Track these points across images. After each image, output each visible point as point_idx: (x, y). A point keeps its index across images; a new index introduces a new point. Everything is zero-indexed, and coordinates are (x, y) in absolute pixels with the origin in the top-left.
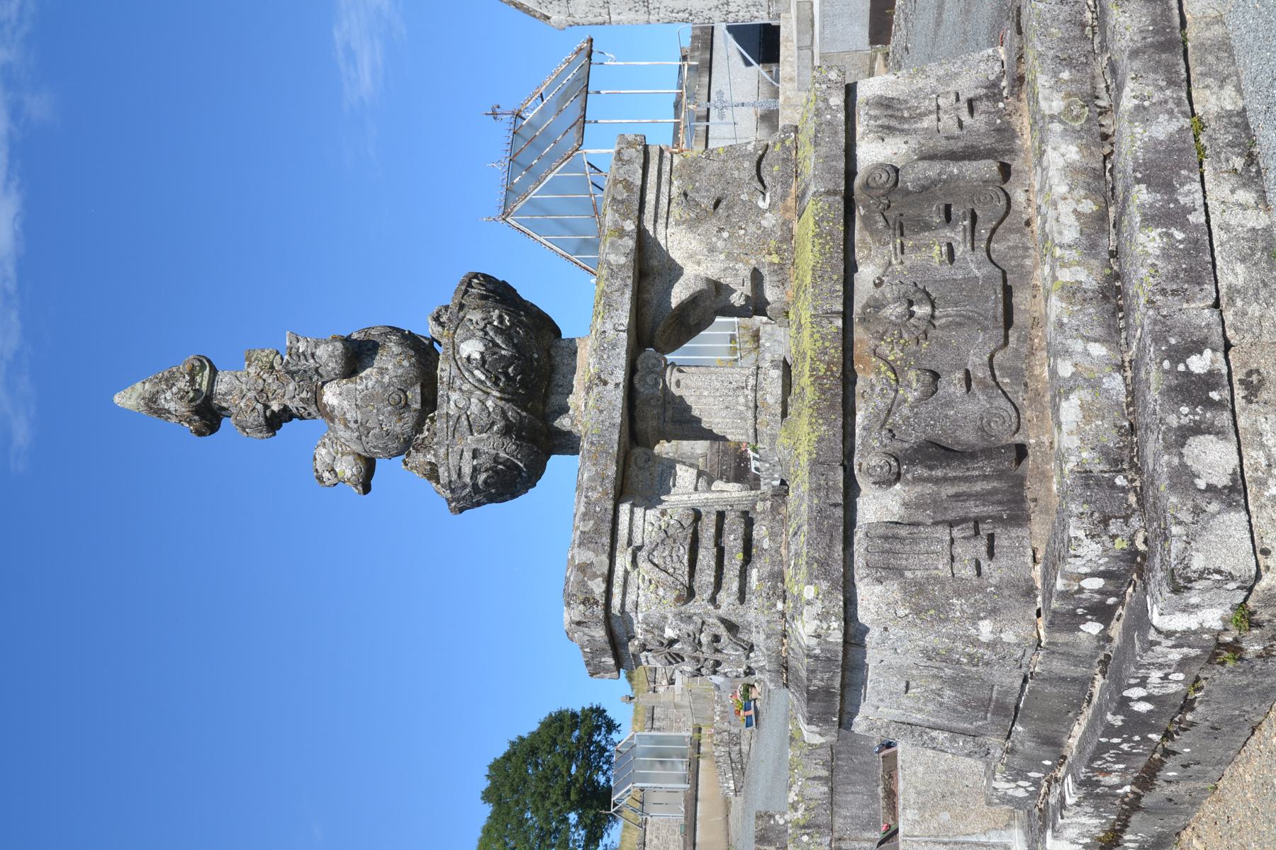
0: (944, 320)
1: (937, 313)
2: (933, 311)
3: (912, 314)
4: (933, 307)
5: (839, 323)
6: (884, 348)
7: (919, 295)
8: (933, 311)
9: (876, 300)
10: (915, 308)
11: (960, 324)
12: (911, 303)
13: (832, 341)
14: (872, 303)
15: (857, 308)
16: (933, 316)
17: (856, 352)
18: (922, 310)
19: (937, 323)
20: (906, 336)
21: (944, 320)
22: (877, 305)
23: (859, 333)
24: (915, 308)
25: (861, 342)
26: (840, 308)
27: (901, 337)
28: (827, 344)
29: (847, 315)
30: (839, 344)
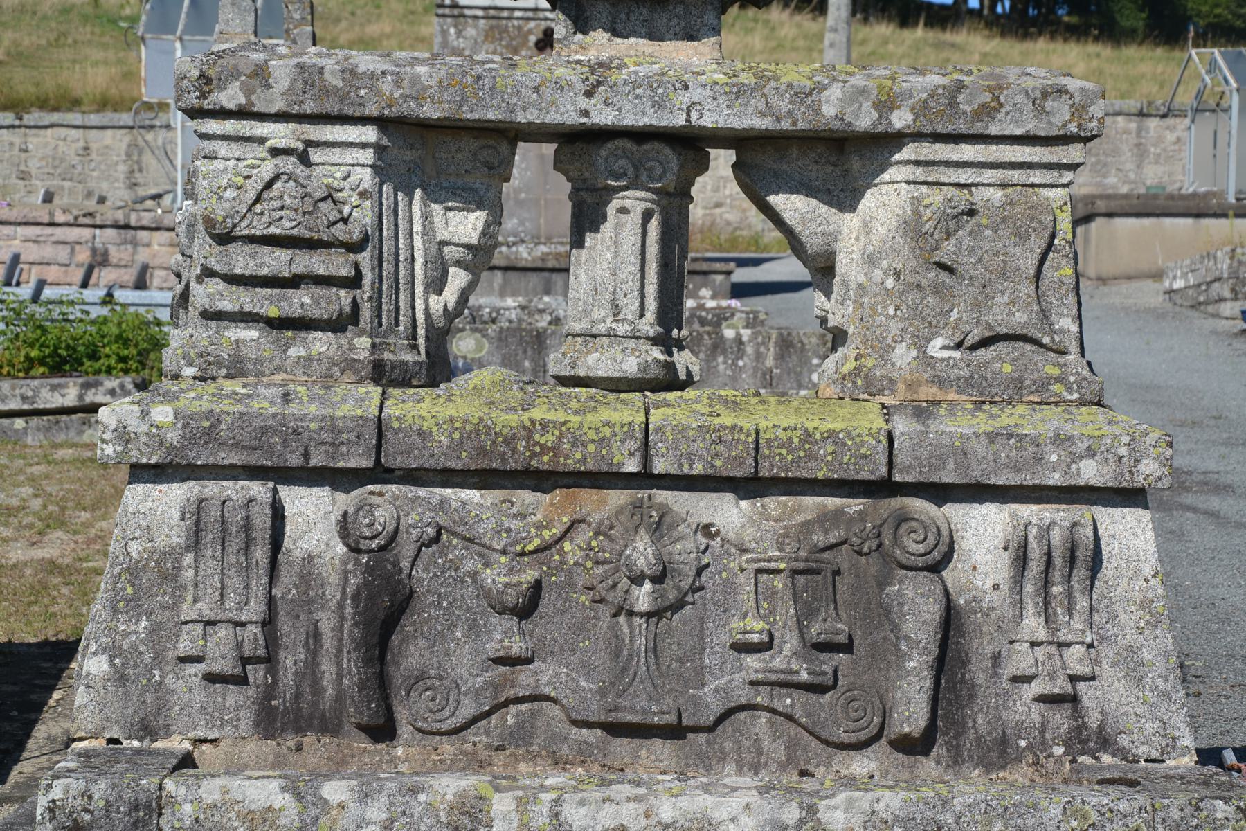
0: (626, 630)
1: (638, 620)
2: (642, 615)
3: (637, 580)
4: (648, 615)
5: (632, 466)
6: (583, 535)
7: (672, 595)
8: (642, 615)
9: (673, 526)
10: (648, 586)
11: (617, 654)
12: (658, 580)
13: (598, 456)
14: (668, 519)
15: (663, 496)
16: (631, 614)
17: (584, 494)
18: (643, 598)
19: (622, 619)
20: (600, 570)
21: (626, 630)
22: (661, 527)
23: (618, 498)
24: (648, 586)
25: (602, 502)
26: (659, 467)
27: (597, 563)
28: (591, 448)
29: (646, 478)
30: (591, 465)
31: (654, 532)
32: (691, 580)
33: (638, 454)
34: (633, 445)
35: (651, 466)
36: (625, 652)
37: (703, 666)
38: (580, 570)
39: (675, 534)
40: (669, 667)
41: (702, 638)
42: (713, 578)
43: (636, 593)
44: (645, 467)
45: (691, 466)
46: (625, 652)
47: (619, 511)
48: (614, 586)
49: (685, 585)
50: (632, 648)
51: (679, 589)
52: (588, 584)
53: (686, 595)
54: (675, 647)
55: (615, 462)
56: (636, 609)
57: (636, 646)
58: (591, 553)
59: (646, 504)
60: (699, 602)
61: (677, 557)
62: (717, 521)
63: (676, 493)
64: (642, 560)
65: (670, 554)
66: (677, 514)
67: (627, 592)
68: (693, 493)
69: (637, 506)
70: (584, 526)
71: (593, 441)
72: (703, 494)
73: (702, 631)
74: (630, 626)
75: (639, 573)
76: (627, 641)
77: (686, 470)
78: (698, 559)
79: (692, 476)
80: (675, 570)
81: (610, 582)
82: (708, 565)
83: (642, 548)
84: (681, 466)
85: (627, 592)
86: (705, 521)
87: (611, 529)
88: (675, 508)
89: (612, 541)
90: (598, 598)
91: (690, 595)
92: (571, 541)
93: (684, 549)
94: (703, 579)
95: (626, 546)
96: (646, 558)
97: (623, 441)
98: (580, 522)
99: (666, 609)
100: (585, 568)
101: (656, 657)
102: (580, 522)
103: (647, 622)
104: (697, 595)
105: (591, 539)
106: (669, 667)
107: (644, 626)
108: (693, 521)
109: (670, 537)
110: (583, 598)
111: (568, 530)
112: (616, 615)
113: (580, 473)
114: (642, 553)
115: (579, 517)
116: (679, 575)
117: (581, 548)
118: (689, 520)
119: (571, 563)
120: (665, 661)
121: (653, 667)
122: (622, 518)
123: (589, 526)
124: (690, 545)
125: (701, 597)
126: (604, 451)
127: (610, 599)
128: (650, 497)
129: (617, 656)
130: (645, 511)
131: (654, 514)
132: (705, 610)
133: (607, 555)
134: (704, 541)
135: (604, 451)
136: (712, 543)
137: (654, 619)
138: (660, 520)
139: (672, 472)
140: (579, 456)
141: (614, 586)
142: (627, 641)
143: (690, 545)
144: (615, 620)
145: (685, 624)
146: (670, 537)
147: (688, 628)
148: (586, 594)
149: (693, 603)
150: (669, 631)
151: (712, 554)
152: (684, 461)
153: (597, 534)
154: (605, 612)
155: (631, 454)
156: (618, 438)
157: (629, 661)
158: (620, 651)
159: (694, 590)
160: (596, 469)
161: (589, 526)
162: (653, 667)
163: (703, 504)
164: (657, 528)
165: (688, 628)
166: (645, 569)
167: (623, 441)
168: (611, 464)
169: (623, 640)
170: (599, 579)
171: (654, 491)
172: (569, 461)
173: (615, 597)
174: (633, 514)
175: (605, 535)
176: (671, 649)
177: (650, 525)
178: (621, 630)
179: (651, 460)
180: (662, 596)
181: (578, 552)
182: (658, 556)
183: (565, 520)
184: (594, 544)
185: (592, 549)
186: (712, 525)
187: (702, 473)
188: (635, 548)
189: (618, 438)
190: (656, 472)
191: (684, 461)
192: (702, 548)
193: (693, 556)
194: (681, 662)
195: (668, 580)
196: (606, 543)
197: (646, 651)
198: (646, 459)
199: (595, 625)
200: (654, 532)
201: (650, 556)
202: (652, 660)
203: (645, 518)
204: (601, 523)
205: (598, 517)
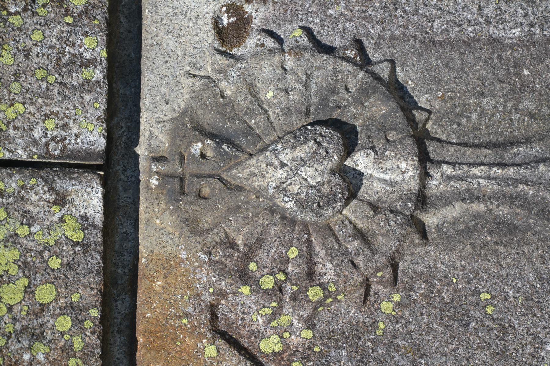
0: (455, 211)
1: (435, 184)
2: (425, 175)
3: (352, 182)
4: (424, 158)
5: (90, 198)
6: (247, 308)
7: (380, 107)
8: (425, 175)
9: (225, 107)
10: (361, 161)
11: (507, 230)
12: (350, 139)
13: (63, 279)
14: (209, 118)
15: (154, 130)
16: (422, 200)
17: (147, 312)
18: (386, 172)
19: (431, 219)
20: (327, 269)
21: (455, 211)
22: (227, 134)
23: (158, 230)
24: (361, 161)
25: (168, 266)
26: (92, 136)
27: (311, 275)
28: (45, 293)
29: (115, 167)
30: (87, 293)
31: (239, 148)
32: (345, 66)
33: (61, 184)
34: (38, 195)
35: (89, 154)
36: (504, 211)
37: (528, 42)
38: (324, 314)
39: (243, 101)
40: (532, 116)
41: (469, 43)
42: (335, 20)
43: (377, 186)
44: (92, 169)
45: (88, 64)
46: (504, 211)
47: (192, 227)
48: (361, 235)
49: (356, 79)
50: (499, 197)
51: (365, 91)
52: (358, 294)
53: (378, 78)
54: (488, 103)
55: (79, 236)
56: (414, 186)
57: (491, 187)
58: (288, 288)
59: (175, 167)
60: (388, 51)
61: (294, 97)
62: (213, 8)
63: (145, 102)
64: (308, 172)
65: (287, 111)
66: (197, 96)
67: (374, 207)
68: (145, 64)
69: (178, 187)
70: (224, 307)
71: (29, 290)
72: (147, 39)
73: (453, 44)
74: (446, 200)
75: (337, 180)
76: (479, 207)
77: (97, 74)
78: (297, 51)
79: (111, 58)
80: (323, 103)
81: (353, 245)
82: (308, 31)
83: (281, 174)
84: (87, 86)
85: (374, 207)
86: (208, 37)
87: (233, 245)
88: (181, 102)
89: (260, 241)
90: (387, 274)
91: (377, 69)
92: (258, 335)
93: (275, 82)
94: (337, 42)
95: (272, 210)
96: (303, 162)
97: (29, 219)
98: (214, 317)
99: (412, 121)
100: (321, 303)
101: (514, 143)
102: (214, 317)
103: (438, 163)
104: (374, 55)
105: (257, 289)
106: (532, 116)
107: (448, 170)
108: (209, 64)
109: (249, 112)
110: (387, 307)
111: (234, 343)
112: (423, 232)
113: (105, 319)
114: (290, 173)
115: (205, 318)
116: (334, 91)
117: (277, 313)
118: (209, 71)
119: (308, 334)
120: (520, 125)
121: (537, 150)
122: (206, 221)
123: (223, 294)
124: (266, 69)
125: (378, 46)
126: (55, 263)
127: (393, 244)
128: (158, 159)
129: (513, 229)
130: (191, 168)
131: (197, 148)
132: (405, 37)
133: (293, 253)
134: (252, 41)
135: (55, 263)
136: (256, 22)
137: (431, 147)
138: (212, 136)
139: (101, 105)
140: (65, 323)
141: (361, 235)
142: (479, 207)
143: (266, 69)
144: (432, 234)
145: (438, 81)
146: (249, 112)
147: (447, 75)
148: (378, 301)
149: (392, 62)
150: (454, 115)
151: (281, 21)
152: (75, 79)
153: (245, 277)
154: (419, 258)
155: (61, 200)
156: (23, 231)
157: (525, 203)
158: (499, 223)
159: (365, 62)
160: (95, 281)
161: (223, 294)
162: (537, 150)
163: (170, 42)
164: (229, 142)
165: (447, 75)
166: (328, 165)
167: (29, 219)
168: (85, 246)
169: (477, 216)
170: (348, 271)
171: (141, 150)
172: (78, 344)
173: (387, 235)
174: (199, 196)
175: (247, 257)
176: (492, 111)
177: (224, 157)
178: (455, 221)
179: (74, 155)
180: (383, 129)
181: (284, 320)
182: (297, 136)
183: (211, 351)
184: (268, 283)
185: (279, 288)
186: (217, 21)
187: (102, 38)
188: (281, 189)
189: (23, 231)
190: (102, 143)
191: (75, 79)
192: (270, 43)
193: (290, 62)
194: (519, 90)
195: (347, 117)
196: (265, 256)
197: (503, 165)
198: (73, 165)
199: (446, 280)
200: (239, 148)
201: (300, 153)
202: (522, 151)
203: (206, 169)
204: (219, 268)
205: (204, 275)
